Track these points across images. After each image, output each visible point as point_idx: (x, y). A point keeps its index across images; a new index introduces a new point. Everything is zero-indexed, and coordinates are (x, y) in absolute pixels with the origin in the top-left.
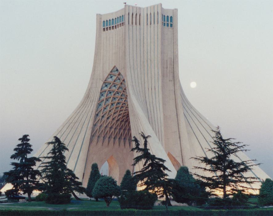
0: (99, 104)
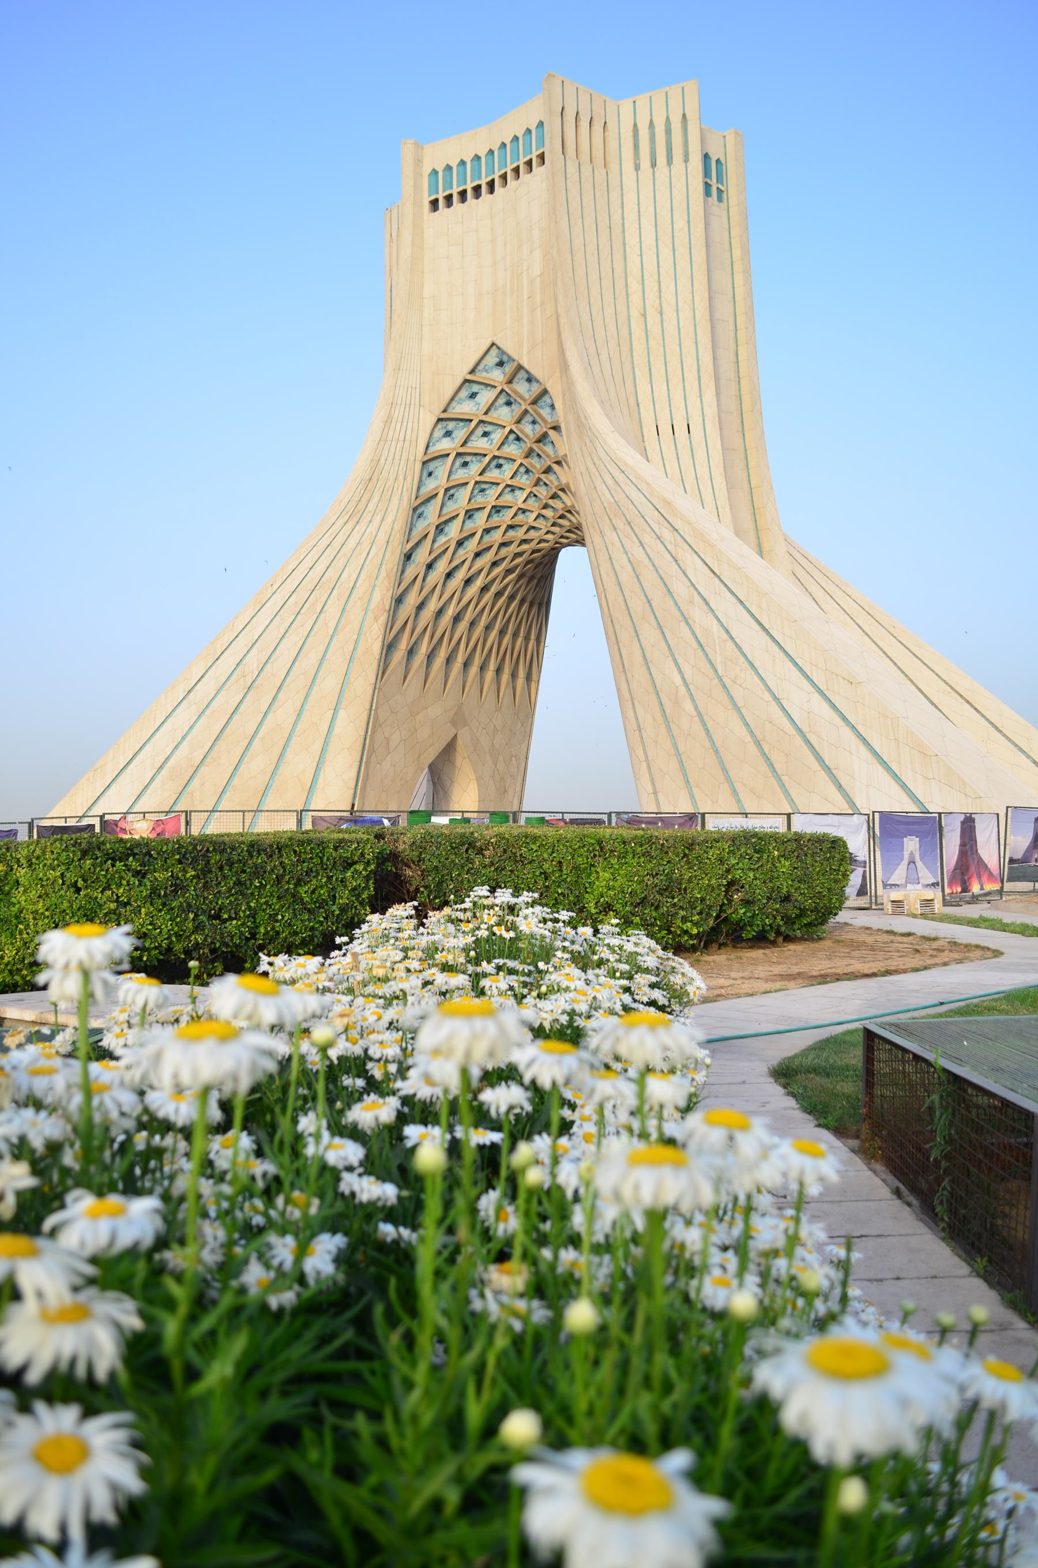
0: (415, 509)
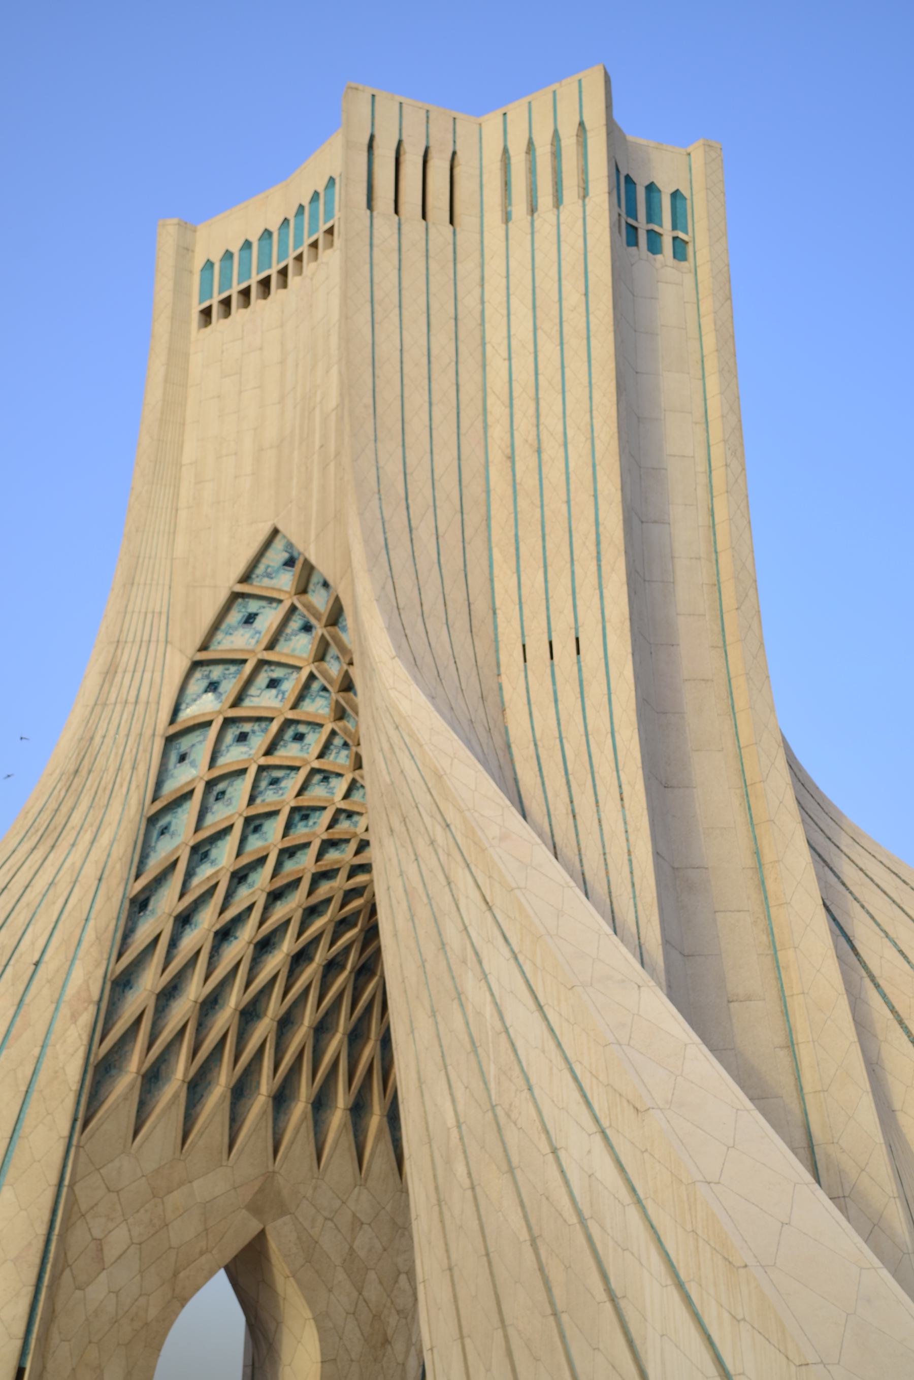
0: (152, 820)
